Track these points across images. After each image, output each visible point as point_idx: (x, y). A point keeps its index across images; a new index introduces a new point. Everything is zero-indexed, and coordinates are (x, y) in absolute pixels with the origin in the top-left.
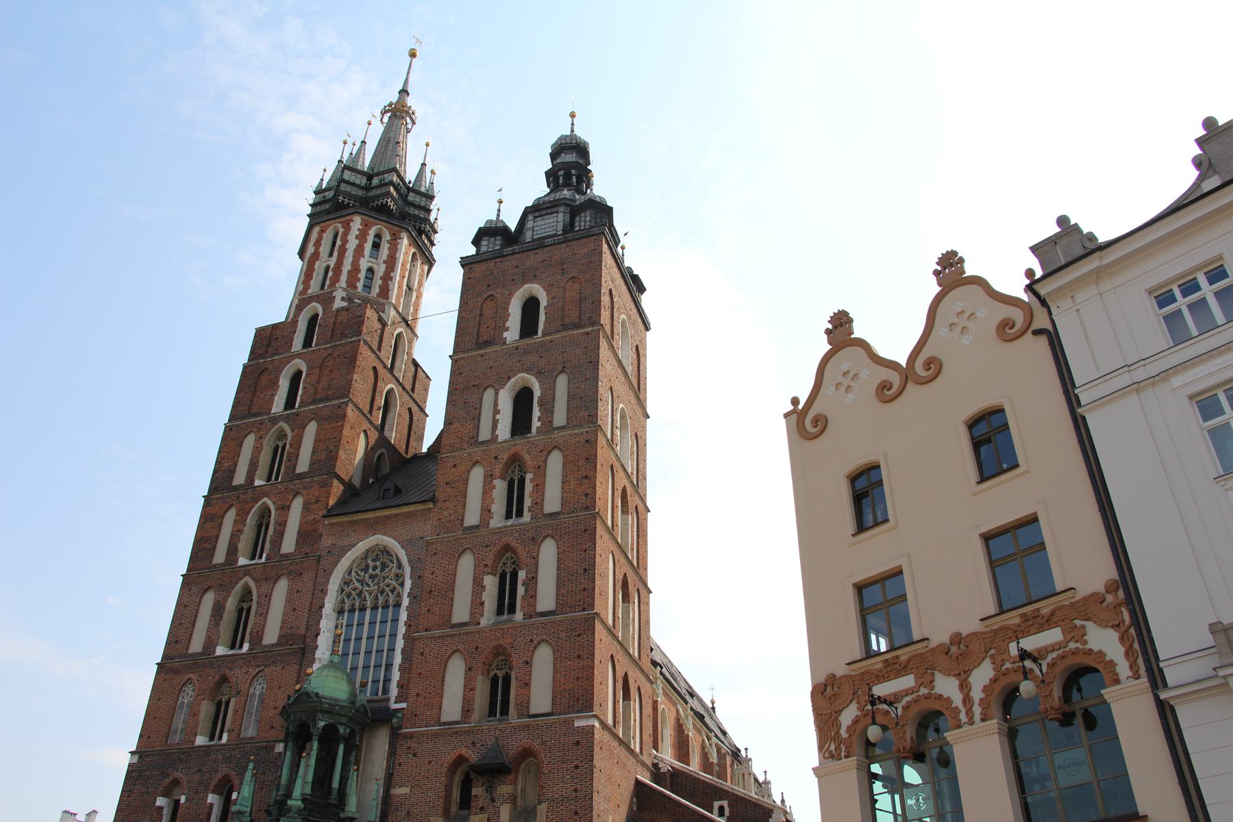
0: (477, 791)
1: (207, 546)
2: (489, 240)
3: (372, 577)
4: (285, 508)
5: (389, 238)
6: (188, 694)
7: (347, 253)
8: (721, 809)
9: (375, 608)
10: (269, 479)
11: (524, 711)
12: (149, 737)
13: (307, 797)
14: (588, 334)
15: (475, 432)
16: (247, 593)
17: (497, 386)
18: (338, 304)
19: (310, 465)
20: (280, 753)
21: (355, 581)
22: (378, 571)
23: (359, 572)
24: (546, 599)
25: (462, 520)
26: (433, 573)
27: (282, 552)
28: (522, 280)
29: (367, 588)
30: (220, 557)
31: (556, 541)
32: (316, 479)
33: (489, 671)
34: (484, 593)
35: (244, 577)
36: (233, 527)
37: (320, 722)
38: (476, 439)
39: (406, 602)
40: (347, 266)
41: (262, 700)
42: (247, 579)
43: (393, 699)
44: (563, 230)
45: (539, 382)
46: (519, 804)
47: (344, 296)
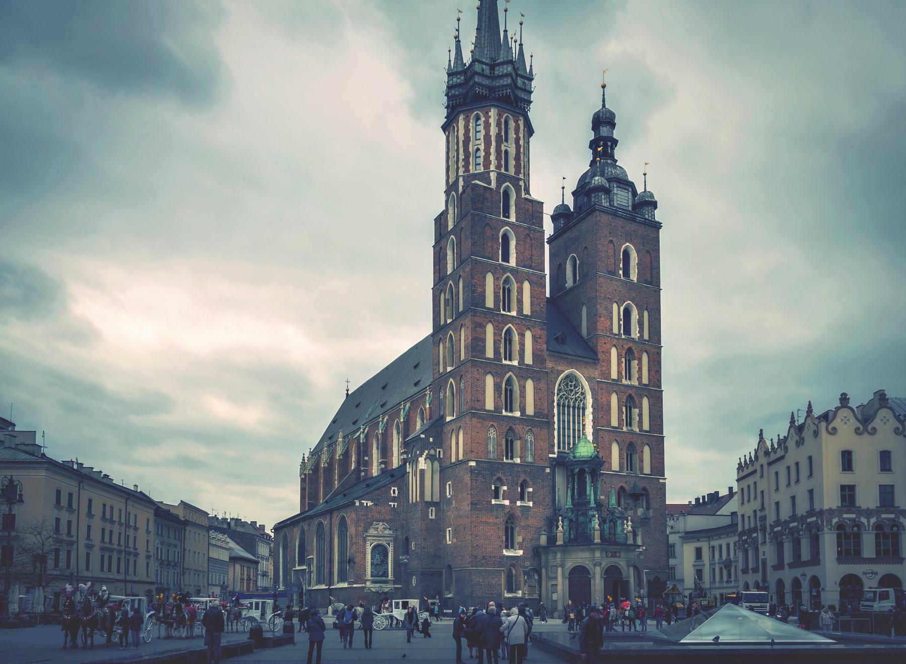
4: (522, 335)
6: (492, 433)
9: (574, 408)
10: (504, 310)
12: (477, 453)
16: (509, 382)
19: (531, 311)
22: (573, 388)
27: (525, 363)
30: (490, 353)
36: (494, 337)
41: (531, 444)
42: (510, 373)
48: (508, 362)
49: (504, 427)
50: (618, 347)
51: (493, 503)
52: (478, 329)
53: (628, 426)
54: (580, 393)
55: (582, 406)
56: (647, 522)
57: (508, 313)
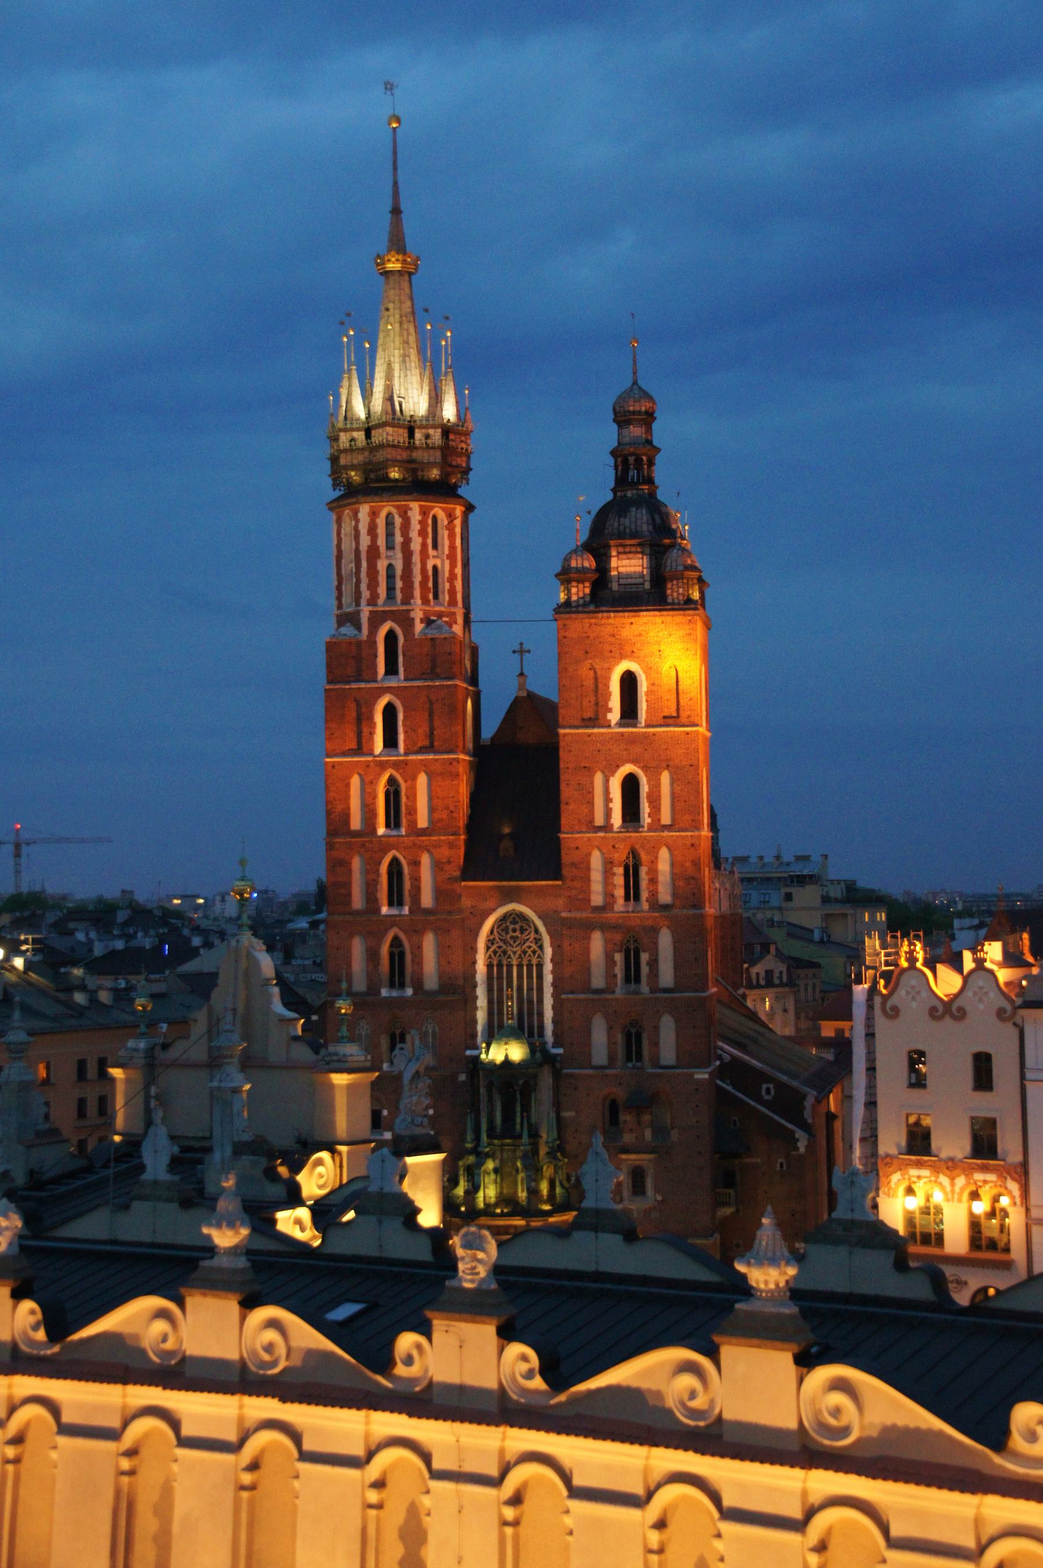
0: (625, 1117)
1: (343, 891)
2: (577, 586)
3: (512, 937)
4: (416, 864)
5: (446, 522)
8: (768, 1091)
9: (520, 966)
11: (656, 1064)
17: (606, 771)
20: (463, 1082)
22: (518, 934)
26: (570, 945)
35: (391, 927)
39: (548, 967)
40: (417, 579)
41: (434, 1037)
44: (651, 581)
45: (646, 776)
48: (394, 911)
55: (534, 962)
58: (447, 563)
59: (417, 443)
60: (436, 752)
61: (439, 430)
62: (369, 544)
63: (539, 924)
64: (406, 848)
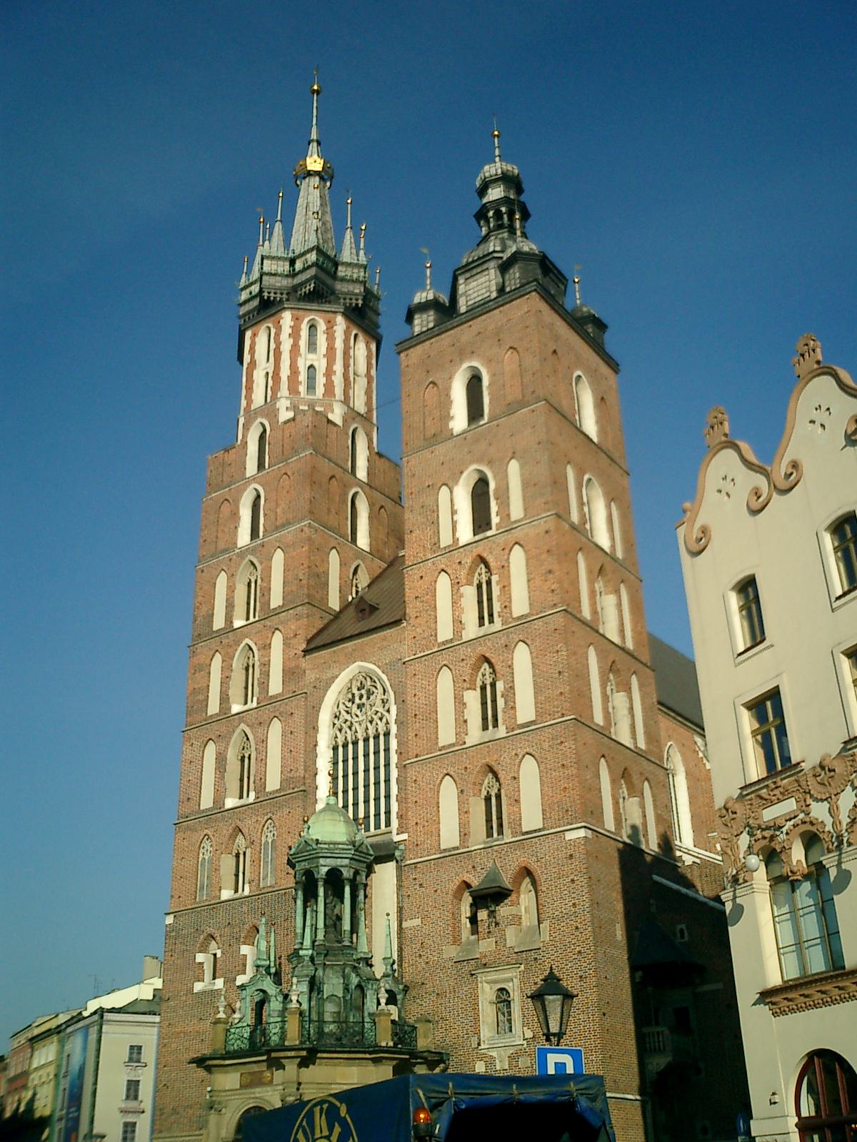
1: (201, 697)
2: (421, 318)
4: (266, 647)
5: (325, 328)
6: (207, 851)
7: (282, 357)
9: (366, 740)
10: (248, 619)
12: (180, 897)
13: (321, 943)
14: (533, 411)
15: (437, 538)
17: (450, 484)
18: (285, 415)
21: (343, 713)
23: (346, 703)
24: (526, 710)
25: (436, 635)
26: (415, 695)
27: (270, 694)
28: (460, 359)
29: (357, 719)
31: (528, 645)
32: (291, 612)
33: (480, 790)
34: (465, 710)
37: (322, 868)
38: (437, 545)
39: (394, 729)
40: (285, 372)
42: (243, 726)
43: (395, 832)
46: (524, 924)
47: (289, 406)
49: (225, 832)
50: (449, 572)
51: (195, 991)
52: (197, 674)
53: (490, 727)
54: (379, 702)
55: (382, 730)
56: (536, 959)
57: (252, 620)
58: (324, 362)
59: (297, 270)
60: (290, 524)
61: (315, 252)
62: (249, 361)
63: (384, 677)
64: (256, 633)
